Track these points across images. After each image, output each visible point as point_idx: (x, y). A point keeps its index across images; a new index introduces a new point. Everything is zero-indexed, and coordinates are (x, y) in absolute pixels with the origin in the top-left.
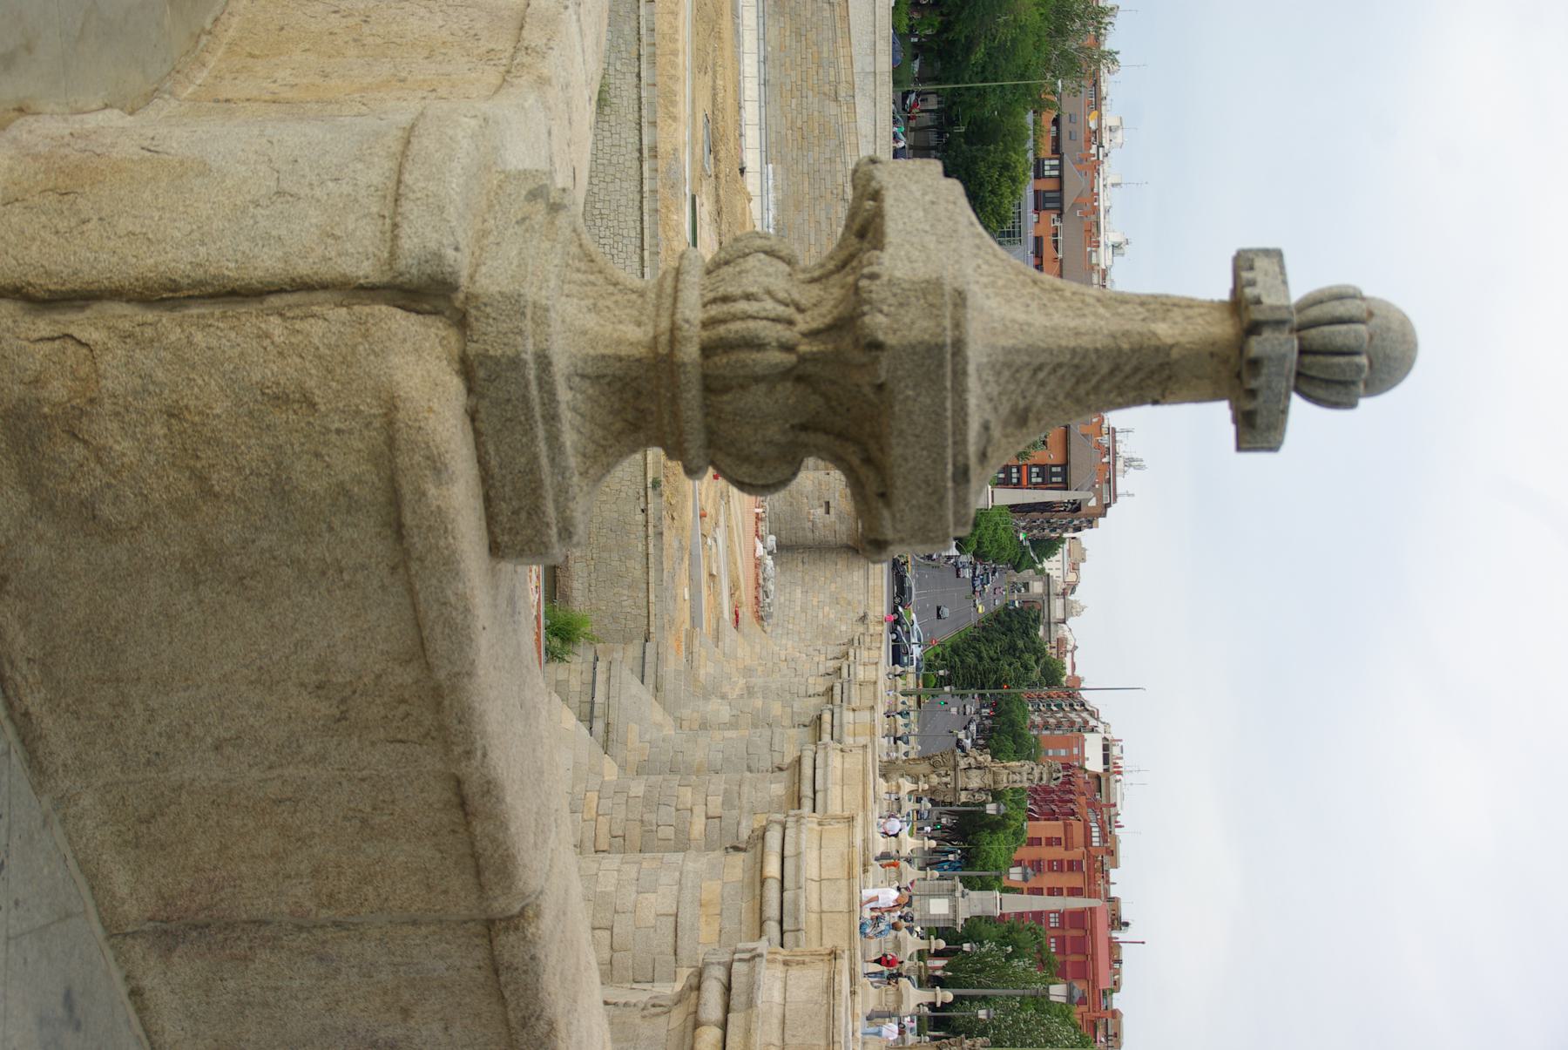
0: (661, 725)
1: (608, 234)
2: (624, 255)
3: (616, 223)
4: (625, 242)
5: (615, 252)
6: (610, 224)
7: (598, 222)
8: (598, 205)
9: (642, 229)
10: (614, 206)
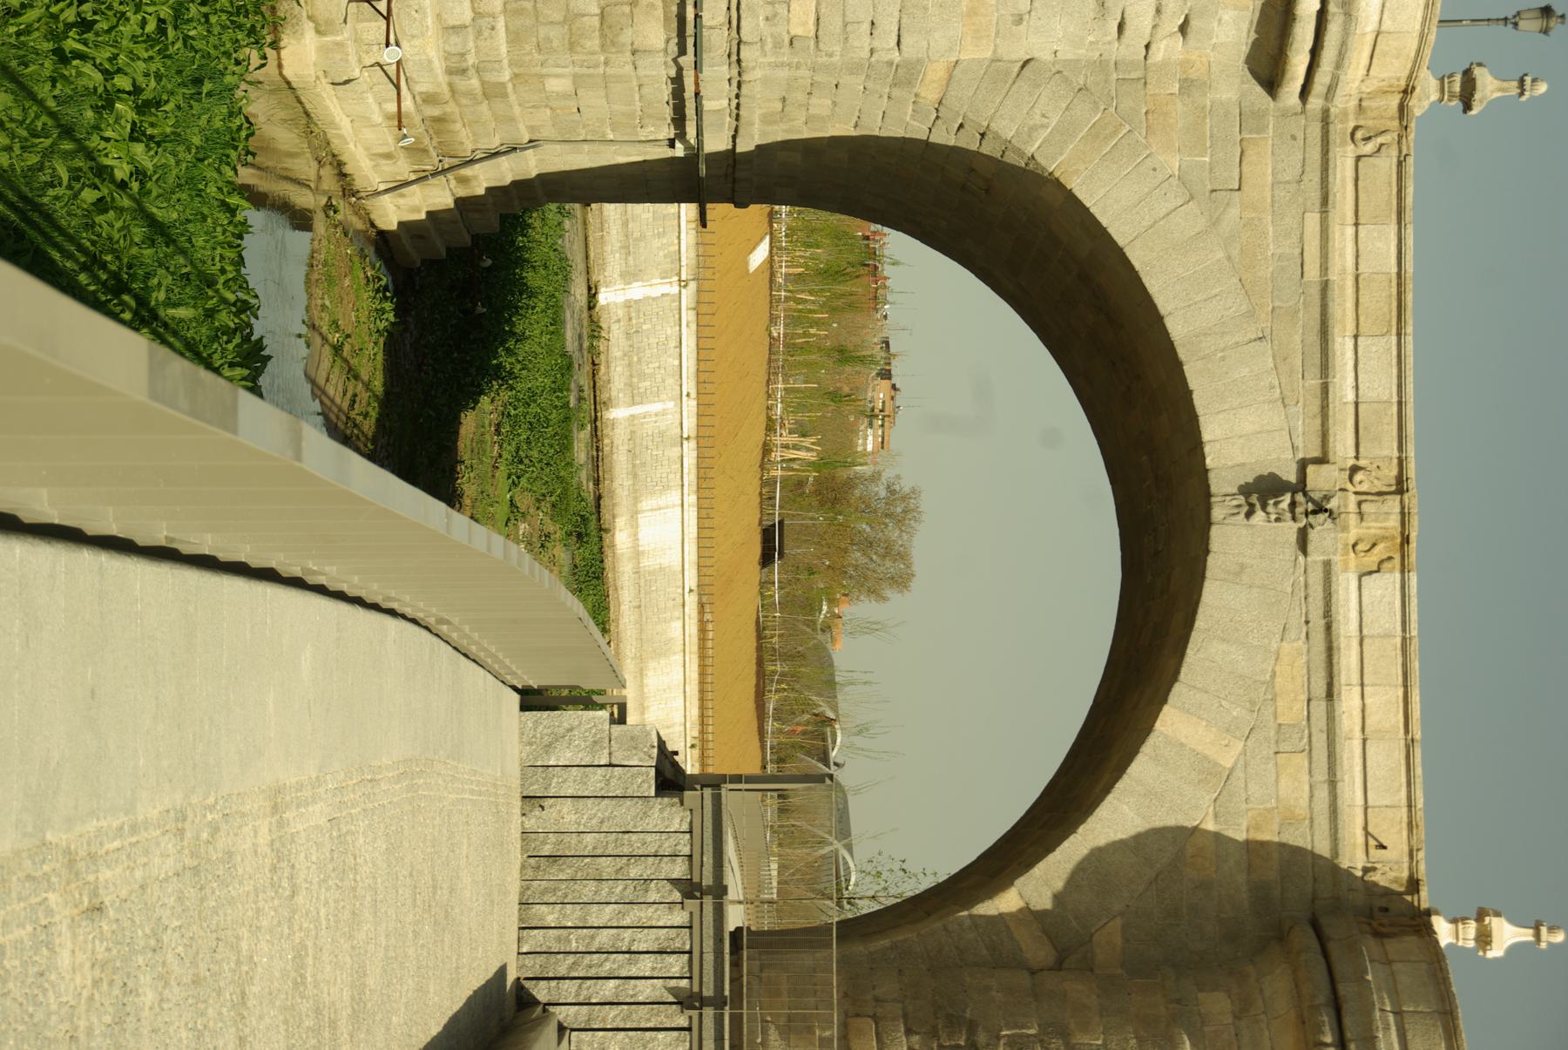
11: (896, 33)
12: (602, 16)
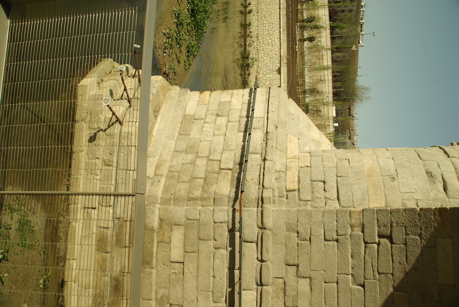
0: (319, 142)
1: (267, 22)
2: (273, 30)
3: (270, 19)
4: (273, 25)
5: (269, 29)
6: (268, 19)
7: (263, 19)
8: (263, 13)
9: (280, 21)
10: (269, 13)
11: (336, 188)
12: (205, 179)
